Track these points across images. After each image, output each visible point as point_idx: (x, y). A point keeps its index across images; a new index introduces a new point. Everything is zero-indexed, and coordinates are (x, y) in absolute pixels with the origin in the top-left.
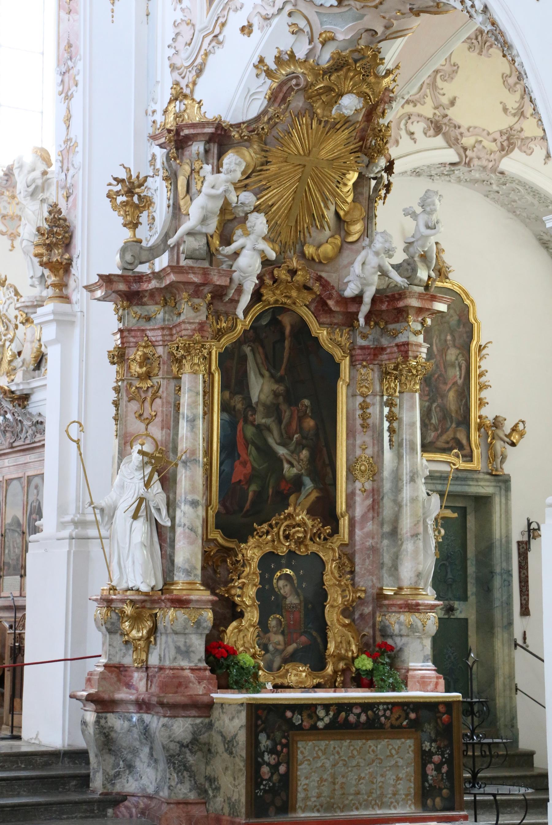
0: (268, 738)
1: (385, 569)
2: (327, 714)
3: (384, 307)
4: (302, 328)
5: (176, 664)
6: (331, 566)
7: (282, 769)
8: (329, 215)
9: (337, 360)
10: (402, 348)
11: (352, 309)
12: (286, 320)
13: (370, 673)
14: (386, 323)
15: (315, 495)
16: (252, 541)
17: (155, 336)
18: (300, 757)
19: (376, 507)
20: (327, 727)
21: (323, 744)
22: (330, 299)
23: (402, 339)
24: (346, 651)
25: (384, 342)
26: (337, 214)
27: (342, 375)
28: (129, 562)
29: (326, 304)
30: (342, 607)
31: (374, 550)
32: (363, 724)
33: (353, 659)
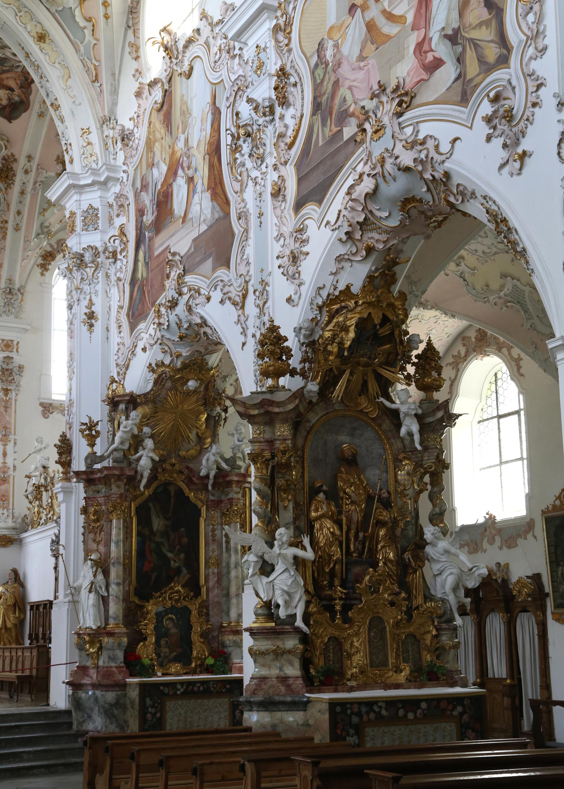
0: (151, 700)
2: (182, 687)
3: (221, 480)
4: (180, 492)
5: (108, 665)
6: (194, 612)
7: (158, 715)
8: (193, 436)
9: (199, 507)
11: (205, 482)
12: (172, 489)
13: (212, 666)
15: (188, 576)
16: (151, 602)
17: (101, 500)
18: (168, 709)
20: (182, 693)
21: (180, 702)
23: (230, 496)
24: (202, 655)
25: (223, 498)
26: (197, 434)
27: (202, 515)
28: (87, 615)
31: (219, 603)
33: (205, 659)
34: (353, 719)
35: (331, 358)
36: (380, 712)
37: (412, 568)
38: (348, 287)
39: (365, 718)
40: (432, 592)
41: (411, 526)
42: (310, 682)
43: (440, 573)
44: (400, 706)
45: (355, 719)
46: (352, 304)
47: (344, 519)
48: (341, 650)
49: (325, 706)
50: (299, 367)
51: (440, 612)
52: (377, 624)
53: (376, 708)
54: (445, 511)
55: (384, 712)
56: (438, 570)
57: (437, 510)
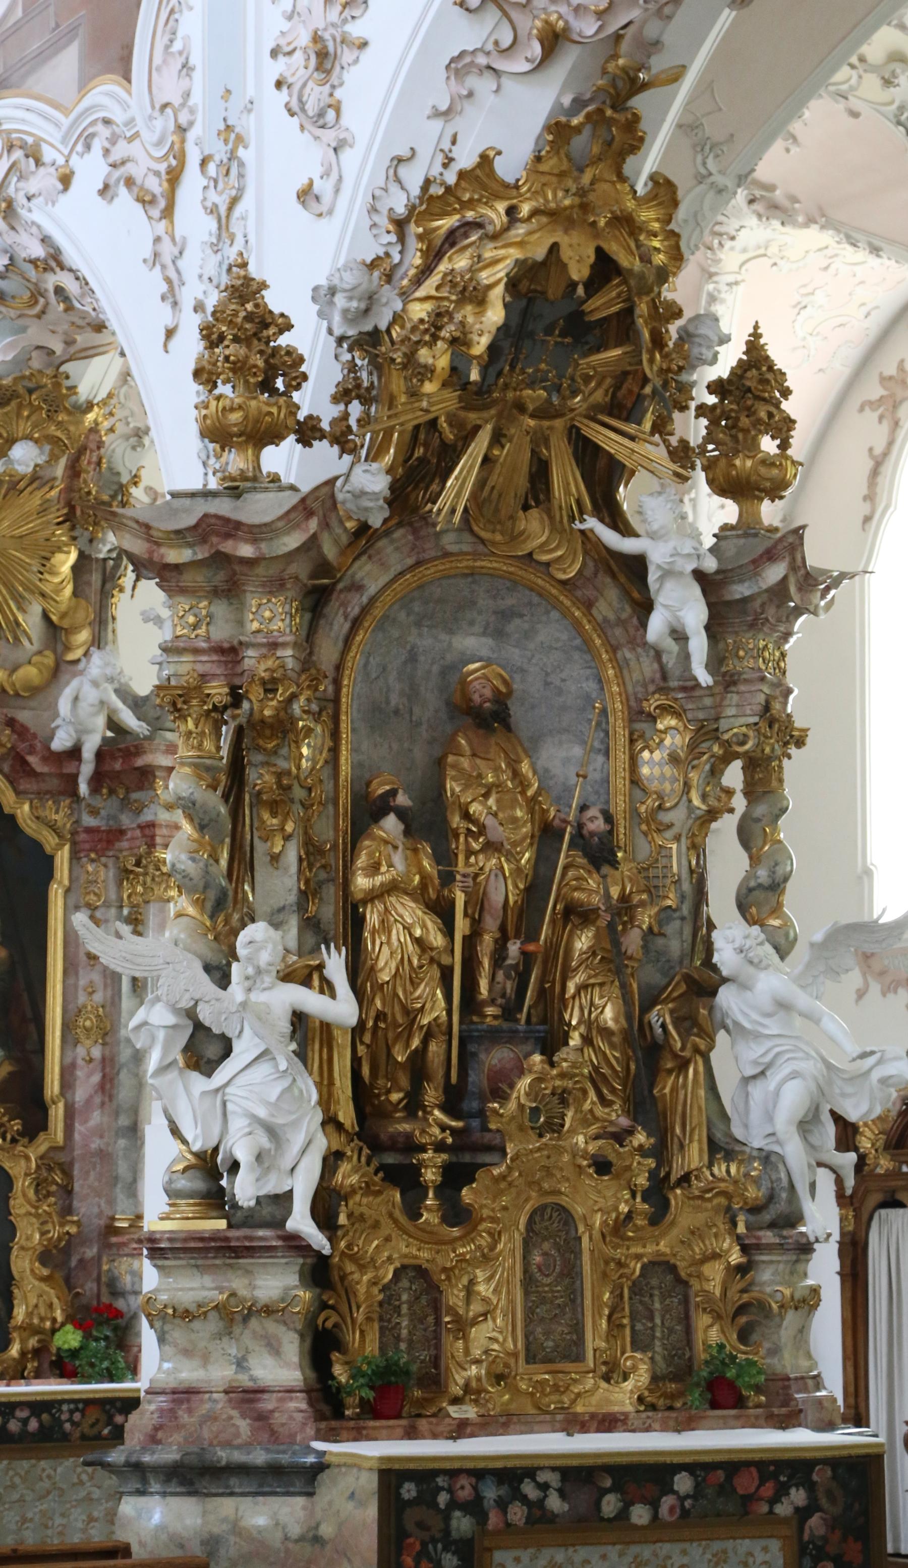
1: (119, 1186)
3: (118, 766)
6: (22, 1185)
8: (31, 621)
9: (48, 849)
10: (147, 831)
11: (69, 769)
13: (74, 1353)
14: (128, 791)
19: (108, 1086)
22: (30, 753)
23: (147, 816)
24: (42, 1319)
25: (126, 820)
26: (46, 616)
27: (57, 875)
29: (25, 763)
30: (40, 1249)
31: (104, 1156)
32: (33, 1434)
33: (54, 1331)
34: (454, 1523)
35: (429, 387)
36: (541, 1503)
37: (675, 1056)
38: (485, 161)
39: (494, 1520)
40: (737, 1131)
41: (677, 923)
42: (329, 1405)
43: (763, 1073)
44: (608, 1483)
45: (462, 1524)
46: (496, 213)
47: (460, 898)
48: (436, 1306)
49: (369, 1482)
50: (328, 413)
51: (752, 1193)
52: (552, 1226)
53: (529, 1489)
54: (786, 879)
55: (554, 1503)
56: (756, 1063)
57: (763, 874)
